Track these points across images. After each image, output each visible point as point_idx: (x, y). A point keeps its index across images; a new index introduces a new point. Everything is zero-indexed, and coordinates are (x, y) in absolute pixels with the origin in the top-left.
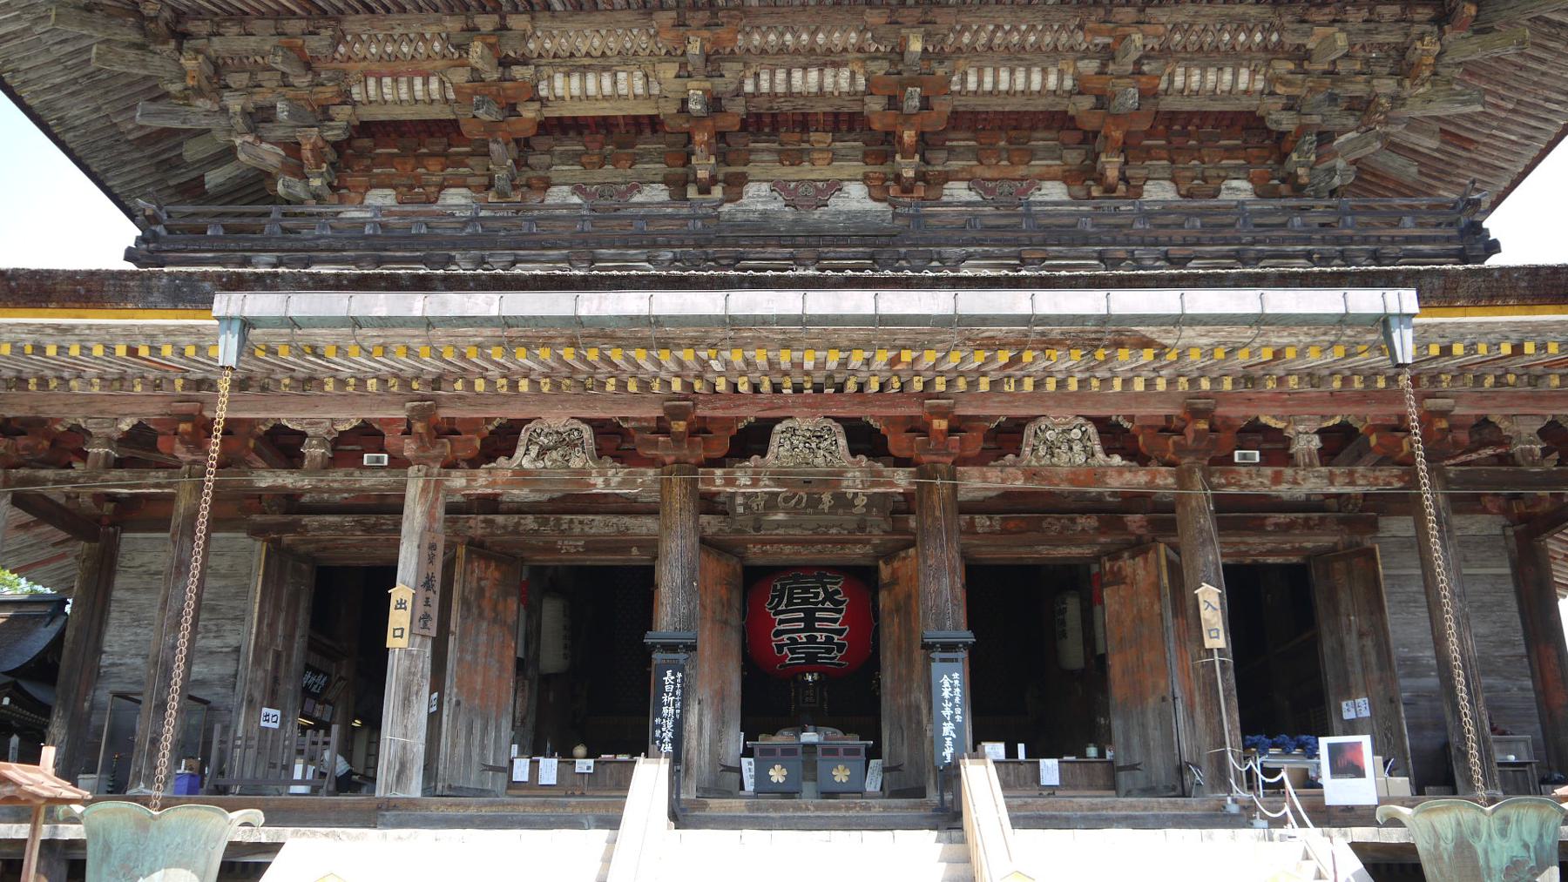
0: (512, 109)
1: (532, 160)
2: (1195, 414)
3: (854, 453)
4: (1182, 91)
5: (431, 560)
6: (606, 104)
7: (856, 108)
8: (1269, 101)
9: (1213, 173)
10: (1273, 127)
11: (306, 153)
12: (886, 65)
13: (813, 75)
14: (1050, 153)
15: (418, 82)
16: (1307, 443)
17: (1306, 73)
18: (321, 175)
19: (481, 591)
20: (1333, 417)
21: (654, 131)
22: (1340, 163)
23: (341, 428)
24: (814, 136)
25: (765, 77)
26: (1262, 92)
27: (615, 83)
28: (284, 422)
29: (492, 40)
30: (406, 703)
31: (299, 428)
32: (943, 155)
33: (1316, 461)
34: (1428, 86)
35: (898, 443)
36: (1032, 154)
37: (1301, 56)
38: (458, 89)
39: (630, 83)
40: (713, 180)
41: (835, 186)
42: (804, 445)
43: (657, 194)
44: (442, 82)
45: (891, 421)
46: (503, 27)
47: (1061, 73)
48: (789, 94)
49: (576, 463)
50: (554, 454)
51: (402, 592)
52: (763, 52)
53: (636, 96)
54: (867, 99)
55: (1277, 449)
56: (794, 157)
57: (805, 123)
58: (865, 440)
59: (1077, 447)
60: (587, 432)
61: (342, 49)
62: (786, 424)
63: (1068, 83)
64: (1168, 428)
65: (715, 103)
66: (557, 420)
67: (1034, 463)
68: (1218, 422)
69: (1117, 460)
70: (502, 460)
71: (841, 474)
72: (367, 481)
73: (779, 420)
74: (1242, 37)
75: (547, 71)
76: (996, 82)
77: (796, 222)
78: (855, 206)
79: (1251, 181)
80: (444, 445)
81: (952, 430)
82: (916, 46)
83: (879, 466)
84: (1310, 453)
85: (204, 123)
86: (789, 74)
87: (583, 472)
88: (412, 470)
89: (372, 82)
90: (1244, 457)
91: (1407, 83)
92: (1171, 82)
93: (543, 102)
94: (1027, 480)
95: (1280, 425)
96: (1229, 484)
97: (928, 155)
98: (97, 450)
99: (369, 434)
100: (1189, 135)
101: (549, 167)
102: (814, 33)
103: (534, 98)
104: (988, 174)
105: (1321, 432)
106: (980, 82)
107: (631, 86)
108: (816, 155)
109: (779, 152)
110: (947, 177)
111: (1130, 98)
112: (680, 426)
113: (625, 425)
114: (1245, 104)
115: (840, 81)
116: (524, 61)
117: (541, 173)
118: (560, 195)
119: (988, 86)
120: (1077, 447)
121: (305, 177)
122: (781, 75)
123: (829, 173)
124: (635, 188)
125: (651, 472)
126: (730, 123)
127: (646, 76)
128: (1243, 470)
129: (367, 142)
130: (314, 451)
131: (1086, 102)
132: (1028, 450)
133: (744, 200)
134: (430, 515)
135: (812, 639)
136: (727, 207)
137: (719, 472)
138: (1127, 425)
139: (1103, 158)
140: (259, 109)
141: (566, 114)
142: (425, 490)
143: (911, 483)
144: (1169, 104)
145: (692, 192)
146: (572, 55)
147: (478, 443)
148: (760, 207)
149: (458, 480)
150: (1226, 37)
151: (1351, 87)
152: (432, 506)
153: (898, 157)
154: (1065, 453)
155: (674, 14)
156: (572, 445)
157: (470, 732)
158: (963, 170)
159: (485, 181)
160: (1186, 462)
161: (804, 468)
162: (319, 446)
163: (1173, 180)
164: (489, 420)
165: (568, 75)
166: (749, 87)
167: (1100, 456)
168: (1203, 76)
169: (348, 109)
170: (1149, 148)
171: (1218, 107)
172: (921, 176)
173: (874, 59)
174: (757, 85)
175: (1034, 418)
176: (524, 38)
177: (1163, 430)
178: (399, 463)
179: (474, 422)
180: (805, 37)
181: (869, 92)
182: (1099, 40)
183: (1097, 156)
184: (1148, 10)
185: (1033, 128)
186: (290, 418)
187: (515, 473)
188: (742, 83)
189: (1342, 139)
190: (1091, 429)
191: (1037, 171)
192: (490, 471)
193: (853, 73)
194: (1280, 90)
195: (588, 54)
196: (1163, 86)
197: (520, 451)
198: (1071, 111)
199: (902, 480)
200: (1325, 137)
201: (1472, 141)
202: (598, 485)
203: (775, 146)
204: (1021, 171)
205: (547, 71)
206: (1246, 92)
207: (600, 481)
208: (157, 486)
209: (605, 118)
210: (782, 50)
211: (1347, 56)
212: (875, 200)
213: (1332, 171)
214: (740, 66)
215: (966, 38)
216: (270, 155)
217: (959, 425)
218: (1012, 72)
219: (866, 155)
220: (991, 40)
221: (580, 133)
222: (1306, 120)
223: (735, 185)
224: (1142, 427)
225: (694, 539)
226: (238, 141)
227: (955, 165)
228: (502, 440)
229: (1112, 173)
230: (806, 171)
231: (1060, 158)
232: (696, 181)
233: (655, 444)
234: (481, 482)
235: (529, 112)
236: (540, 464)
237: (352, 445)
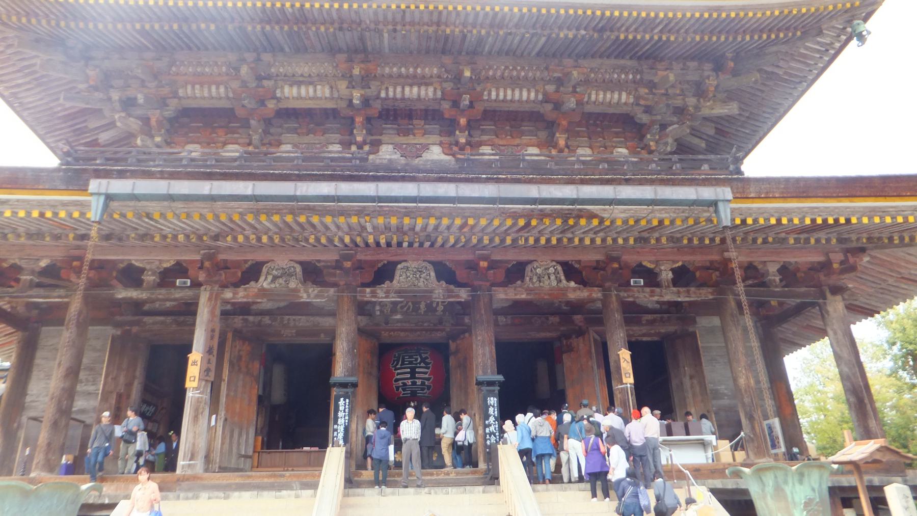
0: (262, 103)
1: (272, 130)
2: (611, 259)
3: (439, 278)
4: (595, 102)
5: (212, 338)
6: (310, 102)
7: (437, 107)
8: (636, 108)
9: (610, 144)
10: (638, 121)
11: (153, 122)
12: (452, 84)
13: (415, 89)
14: (531, 133)
15: (214, 88)
16: (666, 275)
17: (654, 94)
18: (161, 135)
19: (240, 358)
20: (678, 262)
21: (335, 117)
22: (670, 140)
23: (166, 265)
24: (415, 122)
25: (391, 90)
26: (632, 104)
27: (315, 91)
28: (133, 262)
29: (252, 65)
30: (196, 418)
31: (141, 265)
32: (479, 132)
33: (671, 285)
34: (711, 102)
35: (461, 275)
36: (522, 134)
37: (652, 86)
38: (234, 92)
39: (323, 91)
40: (365, 142)
41: (426, 147)
42: (414, 277)
43: (335, 148)
44: (226, 88)
45: (458, 262)
46: (259, 59)
47: (537, 92)
48: (403, 99)
49: (293, 284)
50: (281, 281)
51: (196, 357)
52: (390, 76)
53: (326, 98)
54: (442, 102)
55: (651, 278)
56: (407, 133)
57: (410, 114)
58: (445, 274)
59: (553, 277)
60: (299, 269)
61: (174, 69)
62: (404, 264)
63: (540, 97)
64: (598, 267)
65: (366, 102)
66: (282, 261)
67: (531, 285)
68: (622, 264)
69: (572, 284)
70: (252, 283)
71: (431, 292)
72: (178, 294)
73: (400, 262)
74: (623, 76)
75: (280, 83)
76: (505, 96)
77: (407, 164)
78: (435, 157)
79: (627, 148)
80: (221, 275)
81: (490, 267)
82: (467, 74)
83: (452, 287)
84: (667, 281)
85: (98, 106)
86: (403, 88)
87: (296, 290)
88: (202, 288)
89: (189, 87)
90: (635, 282)
91: (702, 100)
92: (590, 97)
93: (279, 100)
94: (528, 294)
95: (652, 266)
96: (629, 296)
97: (472, 132)
98: (26, 277)
99: (180, 270)
100: (597, 126)
101: (281, 134)
102: (416, 68)
103: (274, 97)
104: (501, 143)
105: (672, 270)
106: (498, 95)
107: (323, 92)
108: (416, 131)
109: (397, 129)
110: (481, 144)
111: (571, 103)
112: (348, 264)
113: (318, 265)
114: (625, 110)
115: (428, 93)
116: (269, 77)
117: (276, 138)
118: (286, 149)
119: (501, 97)
120: (553, 277)
121: (152, 137)
122: (399, 89)
125: (332, 291)
126: (374, 111)
127: (331, 87)
128: (635, 289)
129: (186, 120)
130: (149, 278)
131: (549, 107)
132: (528, 279)
133: (380, 153)
134: (212, 313)
136: (371, 157)
137: (368, 290)
138: (577, 266)
139: (558, 135)
140: (129, 99)
141: (290, 106)
142: (210, 299)
143: (468, 296)
144: (589, 108)
145: (354, 148)
146: (294, 76)
147: (240, 274)
148: (388, 157)
149: (228, 294)
150: (616, 76)
151: (676, 102)
152: (214, 308)
153: (457, 132)
154: (546, 281)
155: (346, 55)
156: (291, 275)
157: (232, 436)
158: (489, 140)
159: (248, 141)
160: (607, 284)
161: (413, 288)
162: (153, 274)
163: (591, 147)
164: (246, 261)
165: (291, 86)
166: (383, 95)
167: (564, 282)
168: (605, 95)
169: (176, 101)
170: (578, 132)
171: (611, 111)
172: (468, 143)
173: (446, 81)
174: (387, 94)
175: (530, 262)
176: (270, 65)
177: (595, 268)
178: (196, 285)
179: (238, 262)
180: (411, 70)
181: (443, 99)
182: (556, 75)
183: (554, 134)
184: (579, 61)
185: (522, 120)
186: (136, 259)
187: (259, 290)
188: (379, 92)
189: (671, 128)
190: (559, 268)
191: (525, 141)
192: (245, 290)
193: (435, 89)
194: (642, 102)
195: (302, 75)
196: (586, 99)
197: (262, 279)
198: (542, 111)
199: (463, 294)
200: (663, 127)
201: (728, 133)
202: (304, 298)
203: (396, 126)
204: (517, 141)
205: (280, 83)
206: (625, 104)
207: (305, 295)
208: (59, 297)
209: (310, 109)
210: (400, 76)
211: (673, 86)
212: (446, 154)
213: (666, 144)
214: (379, 83)
215: (491, 73)
216: (134, 124)
217: (493, 265)
218: (513, 91)
219: (441, 131)
220: (503, 74)
221: (297, 118)
222: (654, 118)
223: (376, 145)
224: (585, 267)
225: (354, 326)
226: (117, 117)
227: (485, 138)
228: (252, 272)
229: (562, 143)
230: (411, 139)
231: (536, 135)
232: (356, 143)
233: (334, 275)
234: (241, 295)
236: (273, 286)
237: (167, 277)
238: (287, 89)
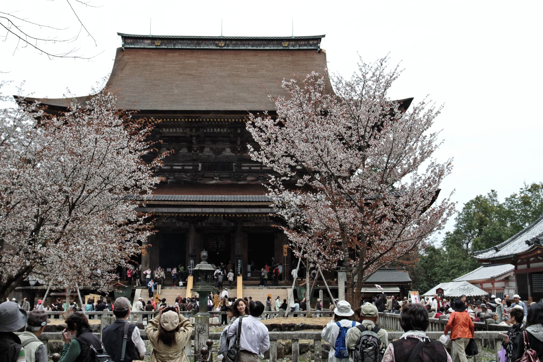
41: (224, 149)
49: (173, 221)
56: (214, 142)
71: (221, 224)
87: (175, 223)
93: (160, 133)
123: (223, 147)
124: (180, 149)
125: (187, 223)
135: (218, 247)
136: (200, 154)
223: (202, 149)
238: (164, 130)
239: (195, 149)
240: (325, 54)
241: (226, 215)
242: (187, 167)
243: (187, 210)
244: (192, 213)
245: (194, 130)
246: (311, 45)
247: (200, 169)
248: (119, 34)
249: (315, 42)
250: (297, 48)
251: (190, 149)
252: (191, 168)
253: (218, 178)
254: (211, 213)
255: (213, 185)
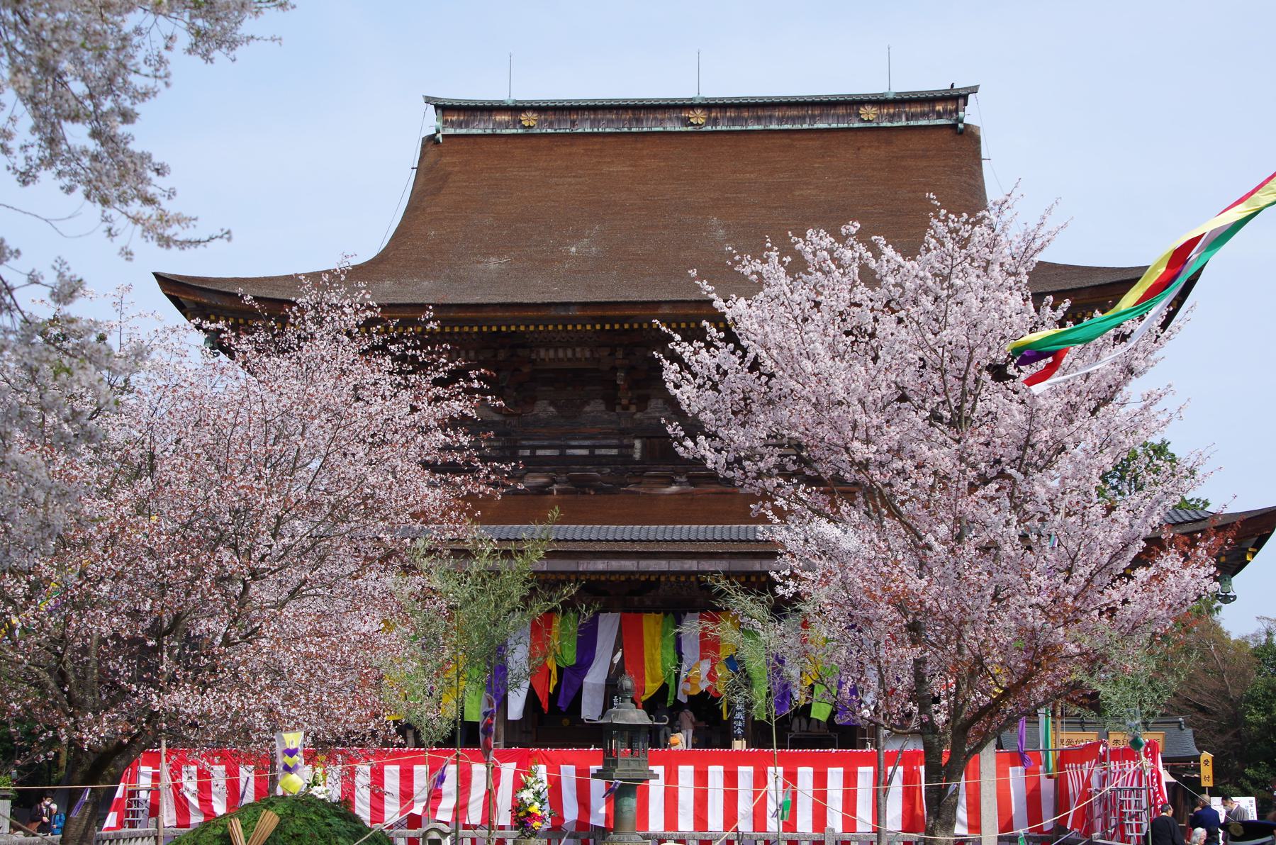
39: (583, 353)
93: (533, 362)
124: (587, 403)
136: (638, 416)
235: (526, 369)
238: (542, 353)
239: (624, 402)
240: (977, 140)
241: (673, 579)
242: (603, 452)
243: (600, 565)
244: (613, 573)
245: (620, 354)
246: (939, 116)
247: (637, 456)
248: (428, 100)
249: (950, 107)
250: (903, 123)
251: (611, 403)
252: (614, 452)
253: (684, 479)
254: (663, 573)
255: (671, 494)
